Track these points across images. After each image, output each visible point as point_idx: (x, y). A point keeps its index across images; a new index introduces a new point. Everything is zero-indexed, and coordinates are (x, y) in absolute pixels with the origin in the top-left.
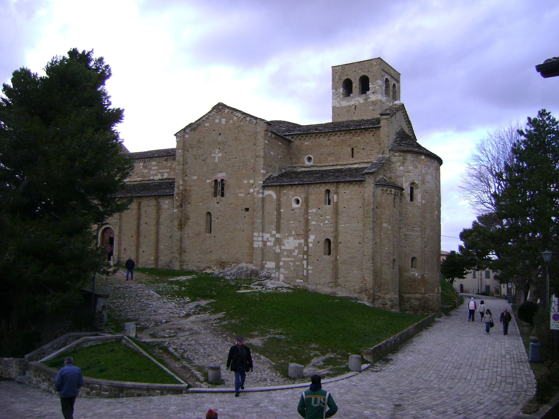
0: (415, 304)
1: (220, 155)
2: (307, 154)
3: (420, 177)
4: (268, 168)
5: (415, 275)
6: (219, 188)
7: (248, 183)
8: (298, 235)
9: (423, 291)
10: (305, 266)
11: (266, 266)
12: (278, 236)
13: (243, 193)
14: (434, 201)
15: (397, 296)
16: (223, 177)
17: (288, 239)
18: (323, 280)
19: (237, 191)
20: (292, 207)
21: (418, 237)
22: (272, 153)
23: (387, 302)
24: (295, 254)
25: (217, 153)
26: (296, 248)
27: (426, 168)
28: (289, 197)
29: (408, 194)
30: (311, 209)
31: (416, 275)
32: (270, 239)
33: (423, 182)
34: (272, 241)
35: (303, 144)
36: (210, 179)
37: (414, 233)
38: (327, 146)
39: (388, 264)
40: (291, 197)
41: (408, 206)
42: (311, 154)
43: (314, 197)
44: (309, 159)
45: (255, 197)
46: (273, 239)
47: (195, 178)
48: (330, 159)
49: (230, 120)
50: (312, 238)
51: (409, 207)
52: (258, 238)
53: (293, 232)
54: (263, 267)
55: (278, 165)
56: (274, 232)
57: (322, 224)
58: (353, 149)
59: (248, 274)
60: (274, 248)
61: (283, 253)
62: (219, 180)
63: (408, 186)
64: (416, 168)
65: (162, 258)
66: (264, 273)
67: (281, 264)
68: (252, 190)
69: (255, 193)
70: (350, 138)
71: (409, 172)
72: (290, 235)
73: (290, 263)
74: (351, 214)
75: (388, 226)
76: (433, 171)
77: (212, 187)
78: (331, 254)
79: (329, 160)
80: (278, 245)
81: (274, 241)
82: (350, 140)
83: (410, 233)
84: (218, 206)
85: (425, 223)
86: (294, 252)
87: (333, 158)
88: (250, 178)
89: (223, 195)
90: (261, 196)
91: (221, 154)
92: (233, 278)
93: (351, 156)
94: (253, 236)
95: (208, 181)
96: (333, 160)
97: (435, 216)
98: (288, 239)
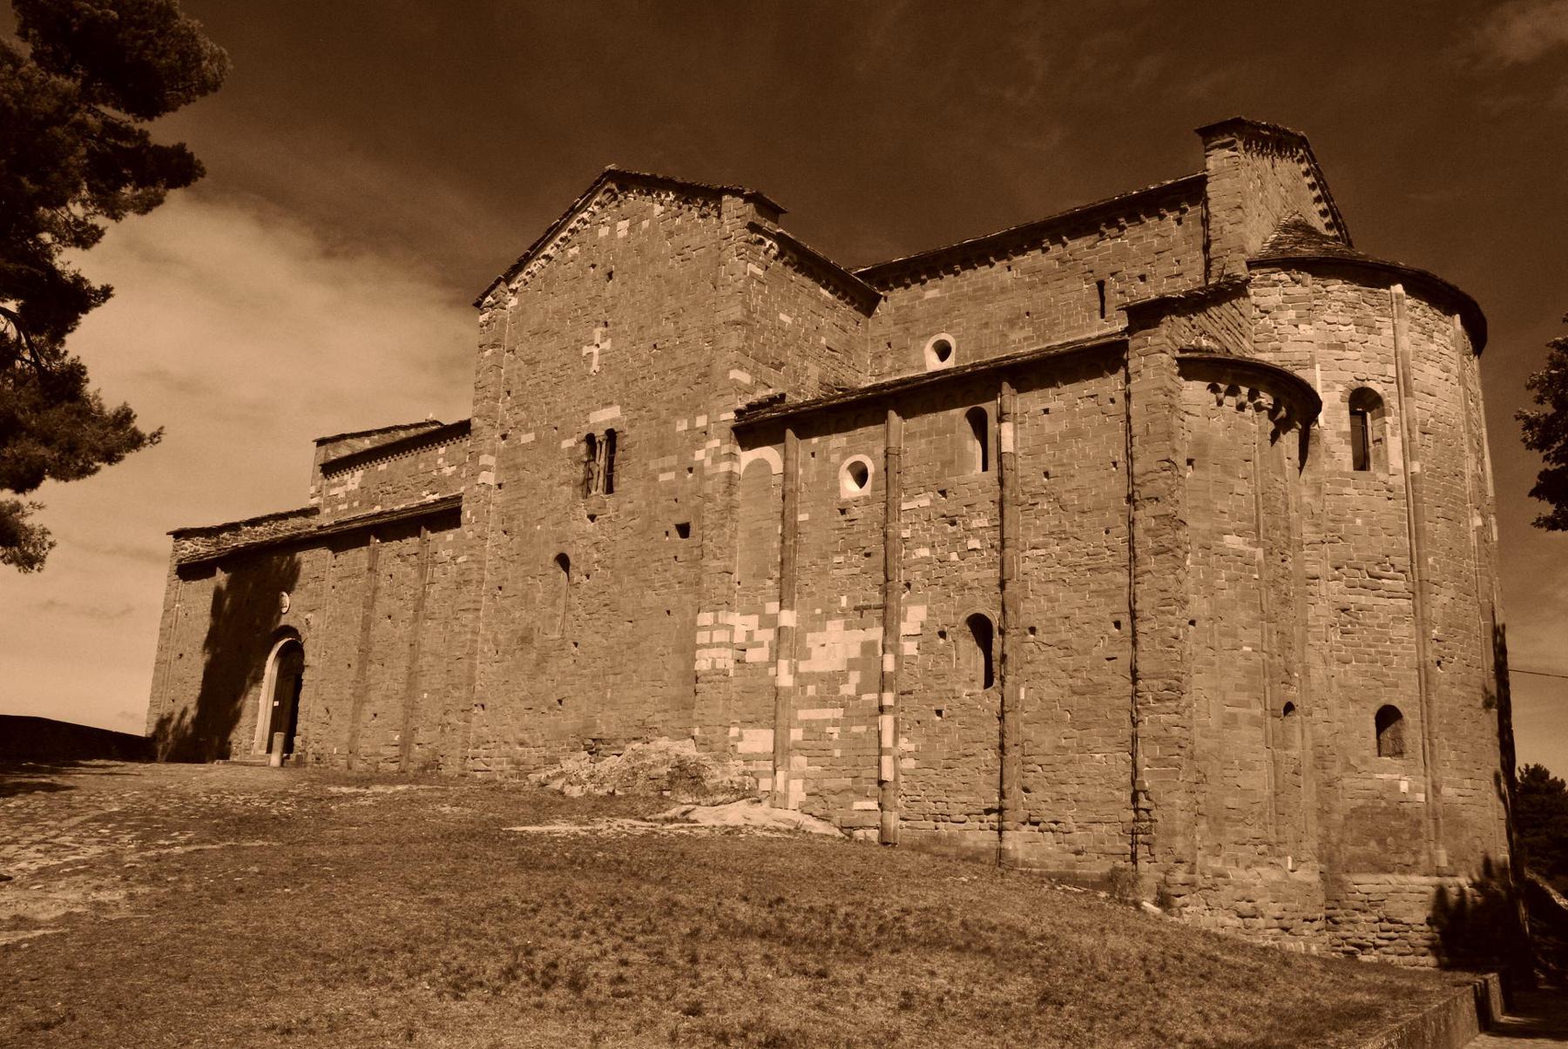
0: (1406, 920)
1: (607, 345)
2: (931, 334)
3: (1391, 370)
4: (764, 369)
5: (1398, 788)
6: (602, 461)
7: (692, 429)
8: (860, 610)
9: (1443, 859)
10: (887, 741)
11: (742, 747)
12: (788, 618)
13: (671, 469)
14: (1462, 473)
15: (1308, 875)
16: (613, 420)
17: (823, 629)
18: (964, 798)
19: (652, 466)
20: (839, 498)
21: (1403, 620)
22: (783, 317)
23: (1259, 902)
24: (848, 690)
25: (597, 341)
26: (852, 664)
27: (1415, 335)
28: (827, 460)
29: (1339, 434)
30: (910, 498)
31: (1404, 787)
32: (759, 635)
33: (1405, 385)
34: (766, 644)
35: (919, 297)
36: (572, 437)
37: (1381, 601)
38: (1003, 290)
39: (1256, 723)
40: (835, 458)
41: (1347, 484)
42: (949, 329)
43: (923, 446)
44: (943, 351)
45: (708, 473)
46: (768, 635)
47: (527, 438)
48: (1016, 335)
49: (641, 219)
50: (914, 617)
51: (1347, 490)
52: (711, 635)
53: (844, 600)
54: (724, 753)
55: (814, 371)
56: (772, 607)
57: (954, 557)
58: (1101, 285)
59: (660, 777)
60: (772, 671)
61: (804, 692)
62: (600, 434)
63: (1337, 401)
64: (1371, 329)
65: (422, 736)
66: (732, 772)
67: (796, 734)
68: (700, 455)
69: (708, 463)
70: (1089, 248)
71: (1341, 346)
72: (828, 615)
73: (829, 729)
74: (1074, 496)
75: (1253, 549)
76: (1446, 352)
77: (577, 463)
78: (996, 682)
79: (1014, 342)
80: (789, 657)
81: (770, 643)
82: (1089, 254)
83: (1363, 600)
84: (590, 525)
85: (1430, 560)
86: (846, 681)
87: (1028, 331)
88: (696, 411)
89: (610, 489)
90: (724, 467)
91: (609, 340)
92: (600, 792)
93: (1097, 314)
94: (694, 628)
95: (567, 444)
96: (1026, 339)
97: (1473, 536)
98: (823, 629)
